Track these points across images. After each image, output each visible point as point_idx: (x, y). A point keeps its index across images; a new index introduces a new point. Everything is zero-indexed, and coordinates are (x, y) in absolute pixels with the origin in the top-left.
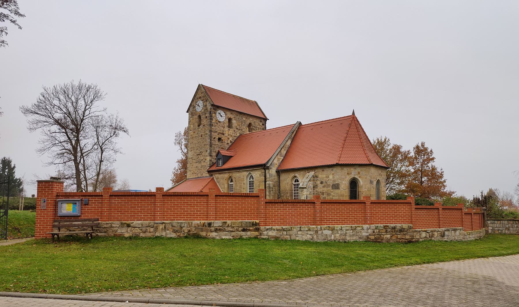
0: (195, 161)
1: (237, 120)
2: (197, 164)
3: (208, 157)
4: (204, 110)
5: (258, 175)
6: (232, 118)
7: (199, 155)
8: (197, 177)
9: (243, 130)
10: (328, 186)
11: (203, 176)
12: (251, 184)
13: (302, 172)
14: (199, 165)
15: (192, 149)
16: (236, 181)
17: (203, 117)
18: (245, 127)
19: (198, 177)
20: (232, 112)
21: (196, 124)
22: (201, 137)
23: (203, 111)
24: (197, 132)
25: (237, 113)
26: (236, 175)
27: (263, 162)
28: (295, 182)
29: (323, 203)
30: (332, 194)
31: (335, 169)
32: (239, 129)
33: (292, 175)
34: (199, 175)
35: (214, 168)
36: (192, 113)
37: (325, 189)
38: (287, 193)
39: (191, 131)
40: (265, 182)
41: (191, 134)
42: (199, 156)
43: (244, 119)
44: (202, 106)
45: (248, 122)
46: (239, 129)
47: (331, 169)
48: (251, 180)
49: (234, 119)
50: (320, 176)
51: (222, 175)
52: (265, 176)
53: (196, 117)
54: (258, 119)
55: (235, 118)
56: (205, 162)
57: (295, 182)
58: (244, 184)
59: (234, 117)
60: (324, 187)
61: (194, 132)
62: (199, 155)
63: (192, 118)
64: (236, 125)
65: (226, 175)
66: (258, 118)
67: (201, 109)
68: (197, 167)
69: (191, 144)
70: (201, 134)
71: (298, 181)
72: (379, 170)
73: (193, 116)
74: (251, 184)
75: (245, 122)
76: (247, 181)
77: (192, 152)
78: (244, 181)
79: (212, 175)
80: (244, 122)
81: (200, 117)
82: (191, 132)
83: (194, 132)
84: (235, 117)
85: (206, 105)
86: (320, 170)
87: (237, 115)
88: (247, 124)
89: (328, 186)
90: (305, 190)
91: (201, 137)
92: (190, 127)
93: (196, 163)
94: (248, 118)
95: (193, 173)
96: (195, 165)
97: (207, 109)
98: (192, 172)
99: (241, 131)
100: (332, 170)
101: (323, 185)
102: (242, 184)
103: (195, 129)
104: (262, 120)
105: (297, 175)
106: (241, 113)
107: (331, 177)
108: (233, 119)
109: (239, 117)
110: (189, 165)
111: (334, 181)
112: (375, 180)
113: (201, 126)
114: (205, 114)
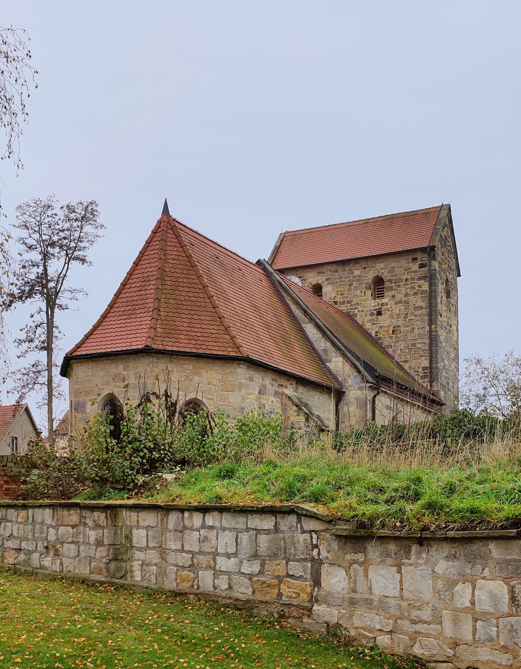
1: (337, 282)
6: (320, 282)
9: (355, 301)
18: (362, 292)
20: (320, 269)
25: (334, 267)
32: (343, 302)
43: (357, 273)
45: (370, 275)
46: (343, 302)
49: (326, 283)
54: (405, 258)
55: (330, 279)
59: (327, 280)
64: (333, 295)
66: (402, 256)
72: (113, 366)
75: (359, 279)
80: (357, 281)
84: (330, 277)
87: (337, 271)
88: (367, 283)
94: (368, 267)
99: (346, 307)
104: (419, 256)
106: (344, 263)
108: (323, 285)
109: (343, 273)
112: (95, 397)
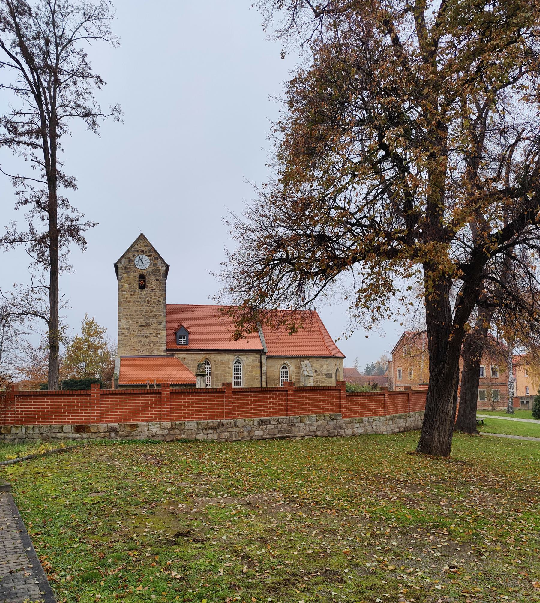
0: (136, 334)
2: (141, 339)
3: (162, 332)
4: (153, 270)
5: (251, 361)
7: (143, 326)
8: (140, 354)
10: (323, 374)
11: (153, 354)
12: (238, 369)
13: (293, 360)
14: (146, 341)
15: (129, 316)
16: (216, 365)
17: (149, 278)
19: (144, 356)
21: (137, 285)
22: (148, 303)
23: (150, 270)
24: (139, 296)
26: (215, 358)
27: (260, 347)
28: (283, 368)
29: (297, 390)
30: (326, 381)
31: (329, 360)
33: (281, 362)
34: (147, 353)
35: (173, 346)
36: (125, 268)
37: (319, 377)
38: (276, 379)
39: (124, 291)
40: (261, 367)
41: (126, 296)
42: (145, 328)
44: (149, 264)
47: (325, 360)
48: (238, 364)
50: (314, 365)
51: (192, 356)
52: (261, 362)
53: (137, 275)
56: (157, 337)
57: (283, 368)
58: (229, 368)
60: (317, 375)
61: (132, 295)
62: (143, 326)
63: (126, 275)
65: (200, 357)
67: (147, 267)
68: (139, 342)
69: (126, 310)
70: (147, 300)
71: (286, 368)
73: (129, 272)
74: (238, 369)
76: (232, 365)
77: (128, 321)
78: (229, 365)
79: (173, 355)
81: (142, 277)
82: (125, 293)
83: (132, 295)
85: (156, 265)
86: (314, 360)
89: (323, 374)
90: (311, 378)
91: (148, 303)
92: (122, 286)
93: (139, 336)
95: (131, 350)
96: (137, 339)
97: (158, 270)
98: (131, 347)
100: (326, 361)
101: (317, 373)
102: (227, 369)
103: (135, 291)
105: (287, 362)
107: (325, 367)
110: (122, 337)
111: (328, 370)
113: (146, 289)
114: (155, 275)
